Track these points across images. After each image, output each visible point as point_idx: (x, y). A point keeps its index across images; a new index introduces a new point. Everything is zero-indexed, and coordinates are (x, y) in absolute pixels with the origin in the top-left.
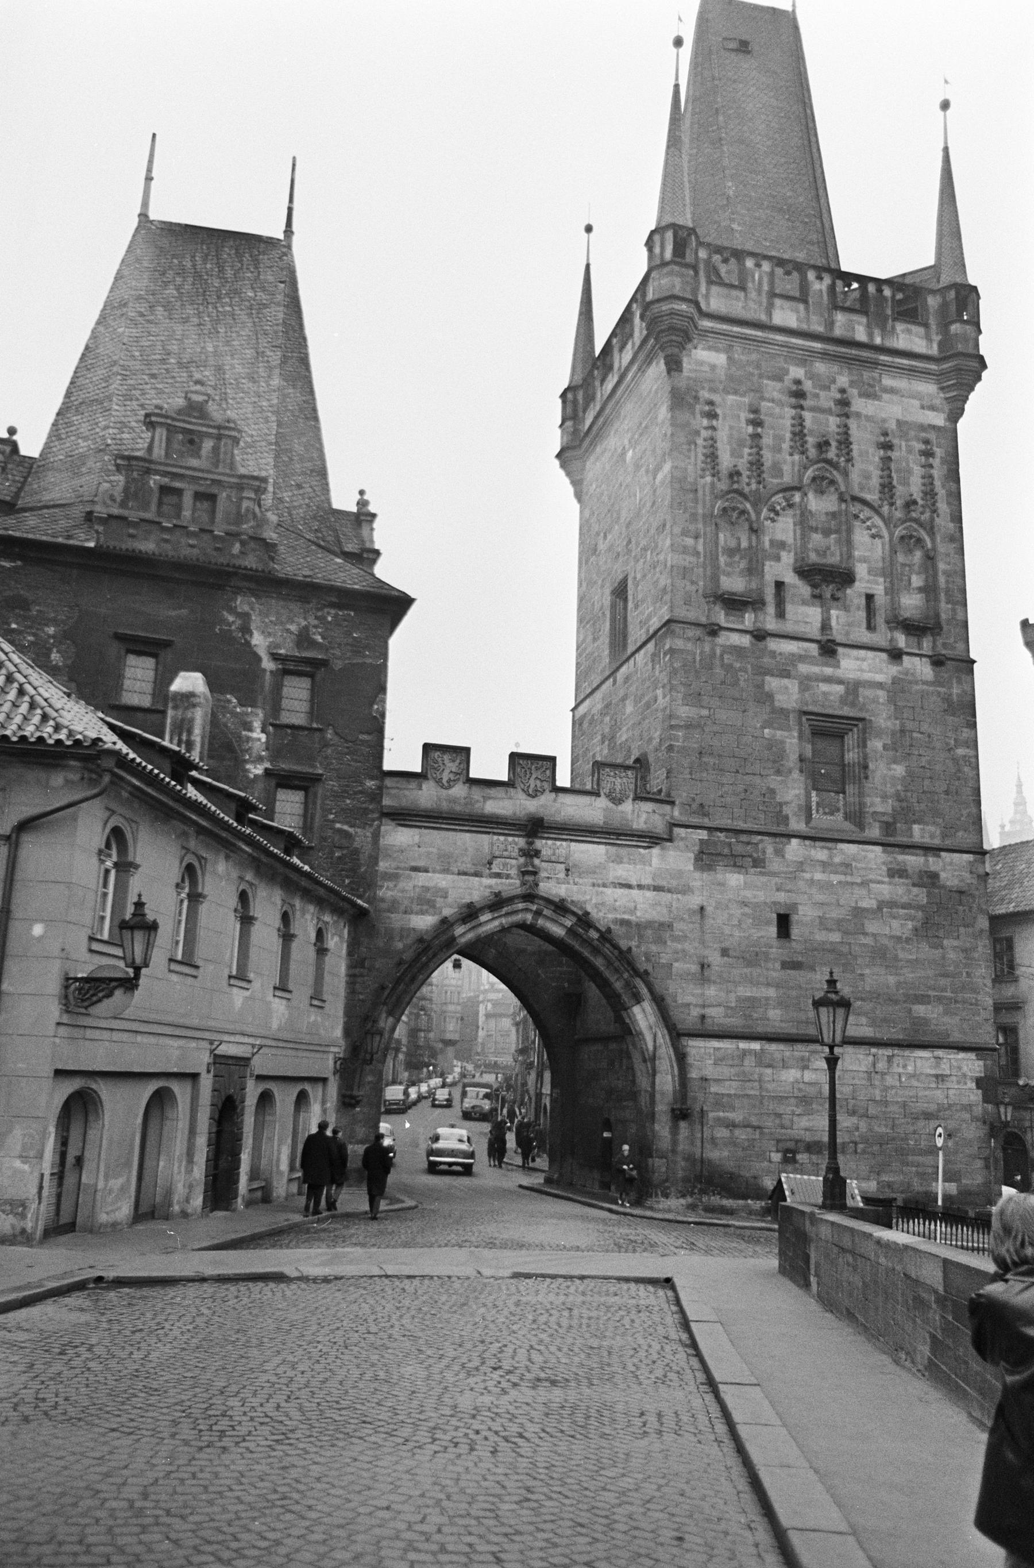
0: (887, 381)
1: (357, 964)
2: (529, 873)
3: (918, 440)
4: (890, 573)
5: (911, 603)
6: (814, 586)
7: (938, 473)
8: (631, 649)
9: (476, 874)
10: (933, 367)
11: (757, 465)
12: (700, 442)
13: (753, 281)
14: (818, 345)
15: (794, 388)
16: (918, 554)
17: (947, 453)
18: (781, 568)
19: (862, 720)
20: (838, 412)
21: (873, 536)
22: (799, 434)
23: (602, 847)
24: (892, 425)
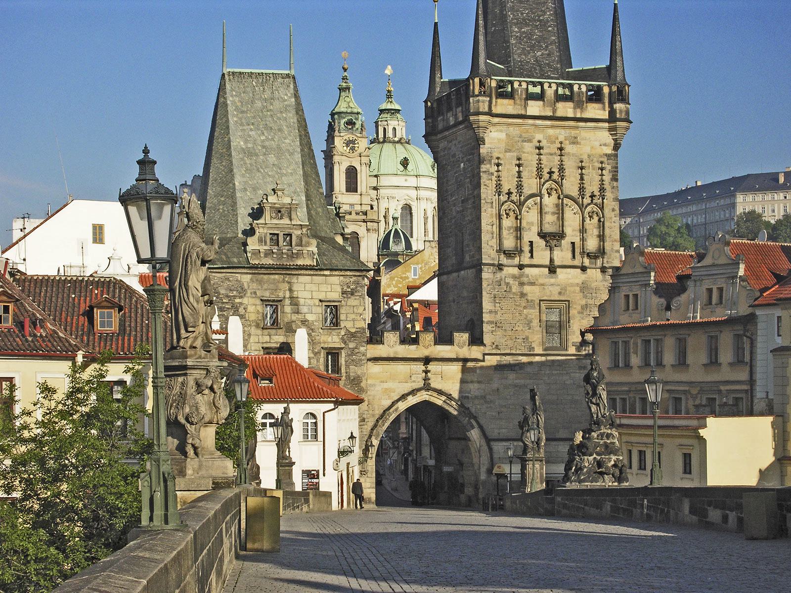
0: (584, 134)
2: (426, 379)
3: (598, 161)
4: (583, 230)
5: (592, 244)
6: (547, 242)
7: (607, 177)
8: (465, 265)
10: (606, 125)
11: (519, 186)
12: (494, 178)
13: (518, 94)
14: (548, 123)
15: (538, 145)
16: (596, 219)
17: (612, 167)
18: (531, 235)
19: (569, 301)
20: (559, 154)
21: (575, 214)
22: (539, 169)
23: (456, 366)
24: (585, 157)
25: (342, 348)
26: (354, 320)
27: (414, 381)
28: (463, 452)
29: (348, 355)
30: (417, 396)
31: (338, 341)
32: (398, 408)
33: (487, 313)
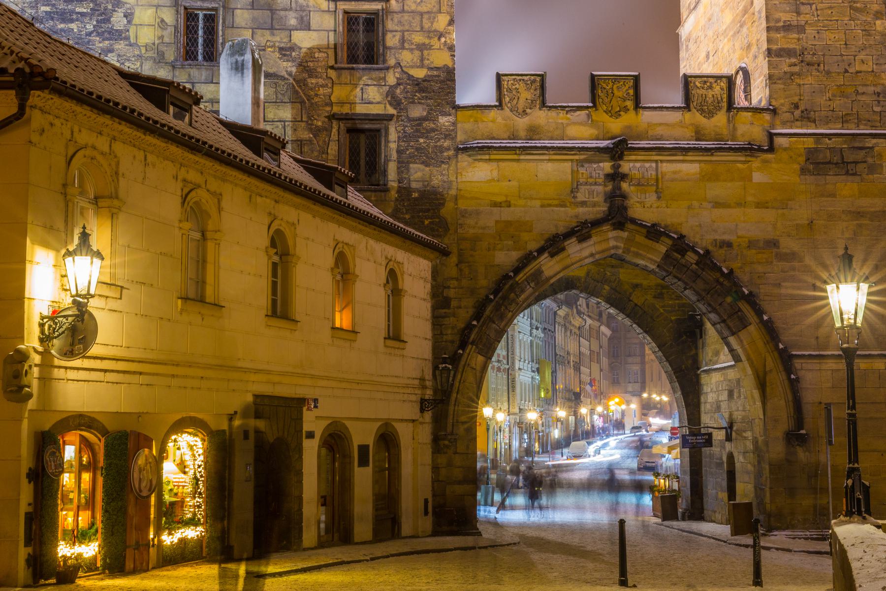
1: (440, 302)
9: (561, 206)
23: (697, 165)
25: (390, 118)
26: (422, 47)
27: (583, 204)
28: (731, 394)
29: (404, 137)
30: (591, 242)
31: (378, 98)
32: (539, 272)
33: (777, 29)
